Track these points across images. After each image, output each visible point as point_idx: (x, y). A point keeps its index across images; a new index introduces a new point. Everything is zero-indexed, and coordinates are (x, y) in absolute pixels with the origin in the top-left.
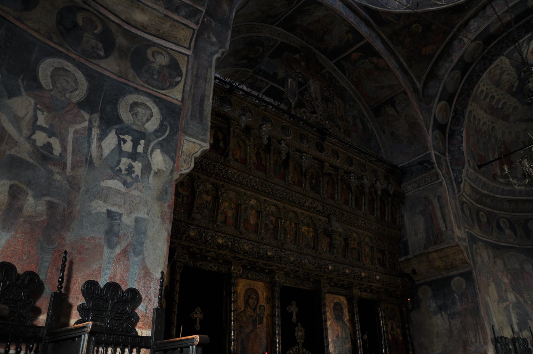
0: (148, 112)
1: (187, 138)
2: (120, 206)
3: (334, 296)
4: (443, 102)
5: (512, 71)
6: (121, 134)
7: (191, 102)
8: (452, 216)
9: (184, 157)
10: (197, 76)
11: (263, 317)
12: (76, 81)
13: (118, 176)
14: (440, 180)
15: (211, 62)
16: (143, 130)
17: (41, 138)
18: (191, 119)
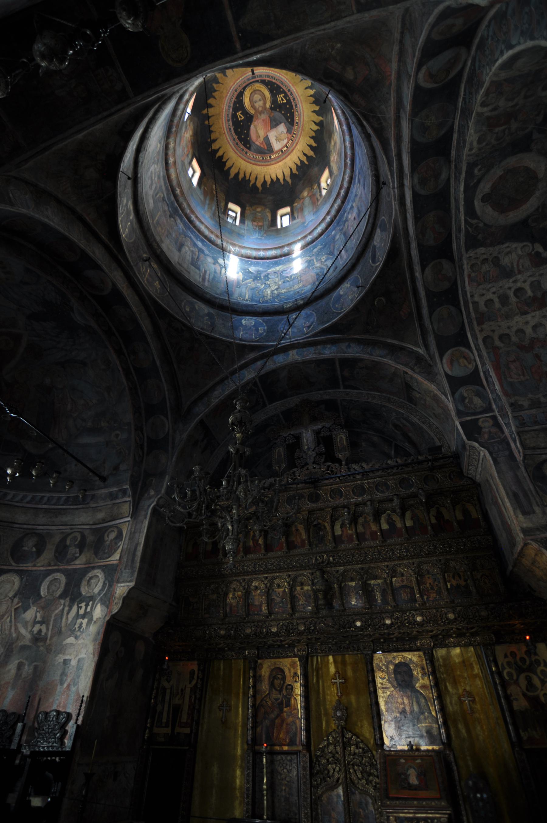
0: (97, 579)
1: (119, 585)
2: (70, 654)
3: (395, 654)
4: (449, 352)
5: (508, 247)
6: (80, 604)
7: (126, 555)
8: (506, 500)
9: (116, 601)
10: (134, 532)
11: (289, 700)
12: (60, 583)
13: (73, 634)
14: (482, 454)
15: (147, 514)
16: (92, 594)
17: (36, 628)
18: (125, 569)
